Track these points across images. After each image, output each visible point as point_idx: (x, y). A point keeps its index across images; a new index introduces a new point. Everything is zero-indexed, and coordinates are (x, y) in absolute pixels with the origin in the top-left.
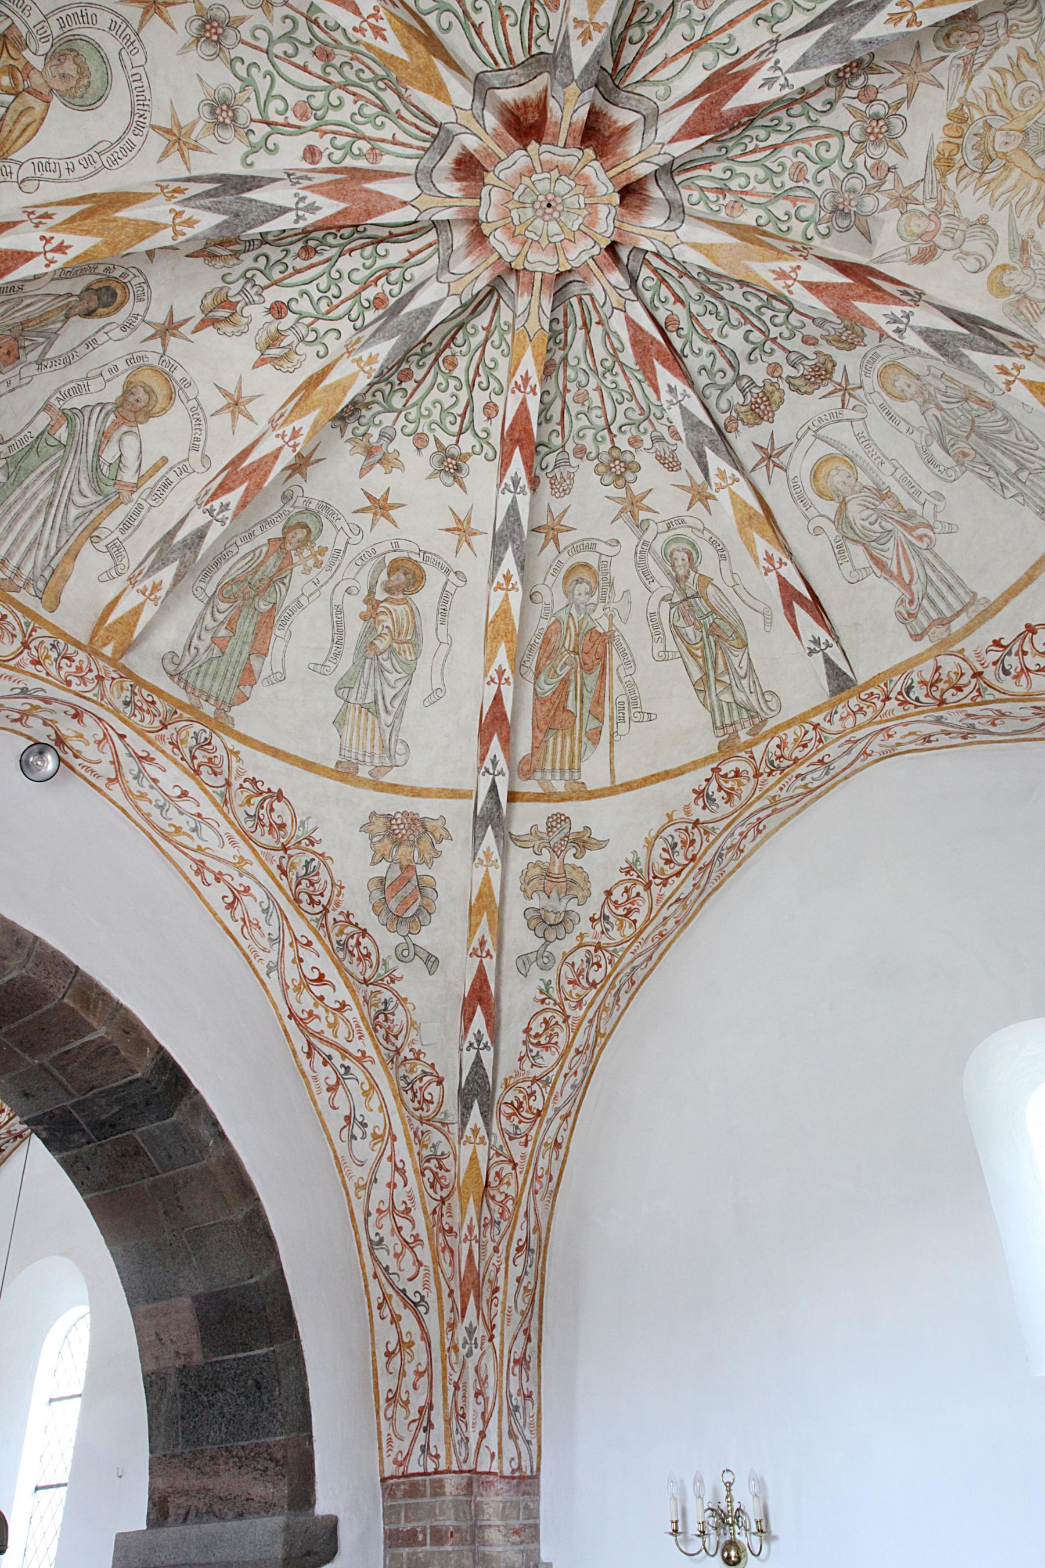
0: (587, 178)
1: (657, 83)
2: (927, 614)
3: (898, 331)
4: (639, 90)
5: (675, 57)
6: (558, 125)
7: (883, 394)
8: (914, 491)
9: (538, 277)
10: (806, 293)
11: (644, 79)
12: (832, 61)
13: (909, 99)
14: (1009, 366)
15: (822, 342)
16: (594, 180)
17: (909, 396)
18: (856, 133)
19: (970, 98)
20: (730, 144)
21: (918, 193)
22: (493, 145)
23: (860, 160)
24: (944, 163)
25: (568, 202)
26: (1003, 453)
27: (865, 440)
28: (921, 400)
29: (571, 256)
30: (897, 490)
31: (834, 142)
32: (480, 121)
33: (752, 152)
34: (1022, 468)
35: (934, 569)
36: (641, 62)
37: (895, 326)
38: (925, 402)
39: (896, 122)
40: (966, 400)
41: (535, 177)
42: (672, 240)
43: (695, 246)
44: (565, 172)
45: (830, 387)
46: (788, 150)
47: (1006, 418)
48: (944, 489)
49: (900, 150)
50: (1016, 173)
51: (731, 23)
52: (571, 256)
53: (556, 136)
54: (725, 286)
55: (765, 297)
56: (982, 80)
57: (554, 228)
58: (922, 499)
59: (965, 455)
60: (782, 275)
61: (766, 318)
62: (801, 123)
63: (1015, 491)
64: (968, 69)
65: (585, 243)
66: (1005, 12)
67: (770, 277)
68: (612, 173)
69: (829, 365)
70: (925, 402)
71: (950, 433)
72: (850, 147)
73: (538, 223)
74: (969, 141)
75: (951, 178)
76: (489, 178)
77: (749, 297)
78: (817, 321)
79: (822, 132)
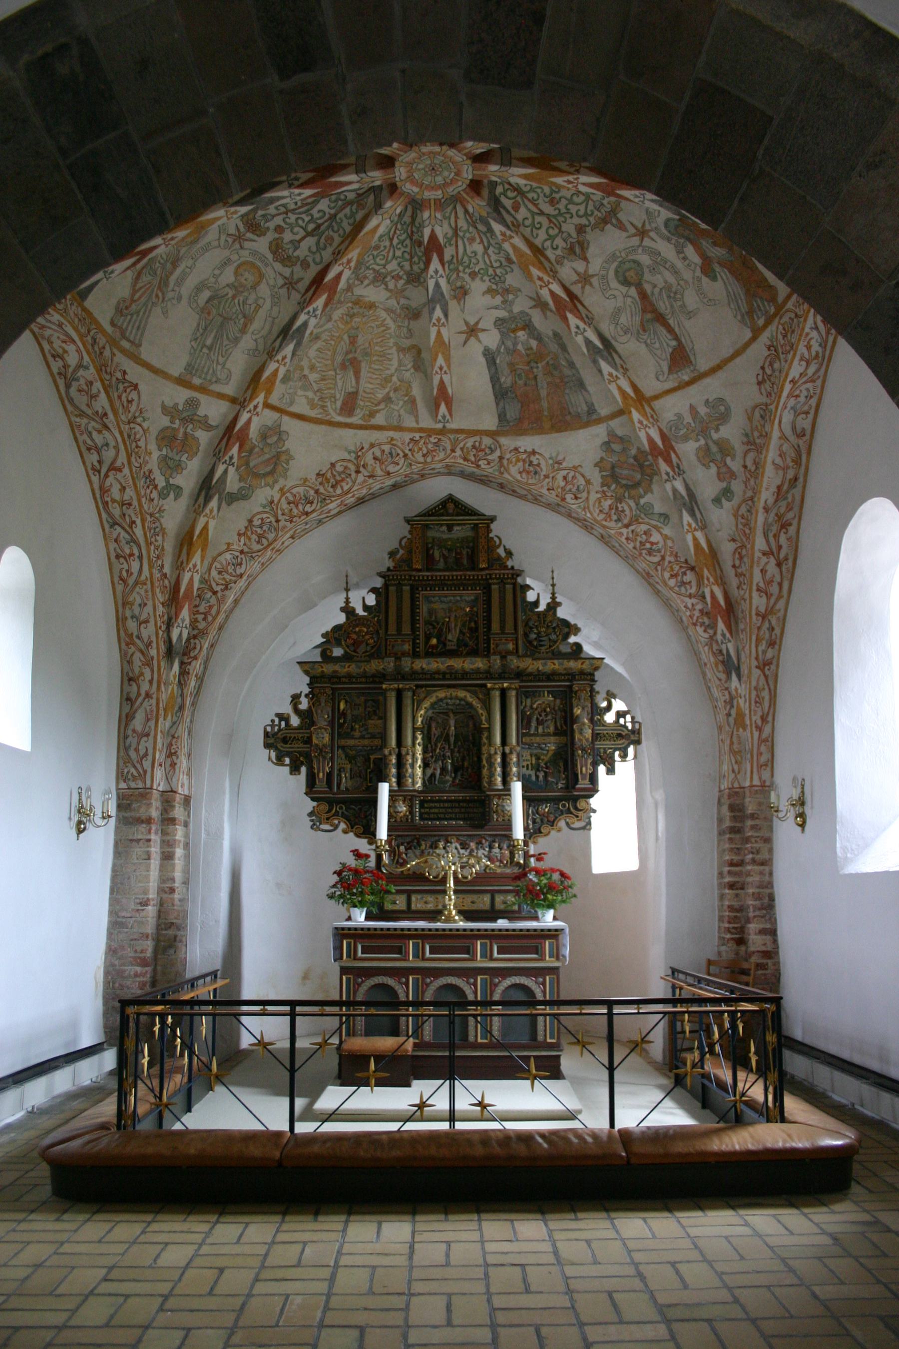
0: (436, 190)
1: (451, 213)
2: (124, 321)
3: (309, 312)
4: (451, 207)
5: (456, 222)
6: (472, 198)
7: (239, 262)
8: (180, 282)
9: (402, 153)
10: (337, 272)
11: (455, 208)
12: (433, 295)
13: (387, 289)
14: (286, 360)
15: (277, 236)
16: (435, 193)
17: (239, 278)
18: (383, 271)
19: (378, 310)
20: (405, 227)
21: (350, 294)
22: (484, 173)
23: (371, 272)
24: (357, 302)
25: (430, 178)
26: (215, 337)
27: (207, 248)
28: (236, 284)
29: (402, 169)
30: (178, 271)
31: (383, 262)
32: (499, 177)
33: (395, 232)
34: (210, 348)
35: (144, 313)
36: (463, 210)
37: (311, 311)
38: (236, 288)
39: (379, 283)
40: (245, 317)
41: (453, 174)
42: (385, 216)
43: (378, 226)
44: (446, 185)
45: (242, 229)
46: (387, 243)
47: (236, 340)
48: (184, 301)
49: (368, 285)
50: (343, 327)
51: (457, 246)
52: (402, 169)
53: (467, 194)
54: (333, 205)
55: (319, 221)
56: (384, 314)
57: (421, 166)
58: (177, 288)
59: (209, 313)
60: (349, 261)
61: (304, 216)
62: (398, 253)
63: (195, 346)
64: (389, 310)
65: (404, 176)
66: (408, 327)
67: (350, 256)
68: (432, 202)
69: (258, 233)
70: (236, 288)
71: (220, 303)
72: (377, 268)
73: (429, 162)
74: (361, 311)
75: (350, 305)
76: (469, 162)
77: (321, 214)
78: (296, 244)
79: (390, 258)
